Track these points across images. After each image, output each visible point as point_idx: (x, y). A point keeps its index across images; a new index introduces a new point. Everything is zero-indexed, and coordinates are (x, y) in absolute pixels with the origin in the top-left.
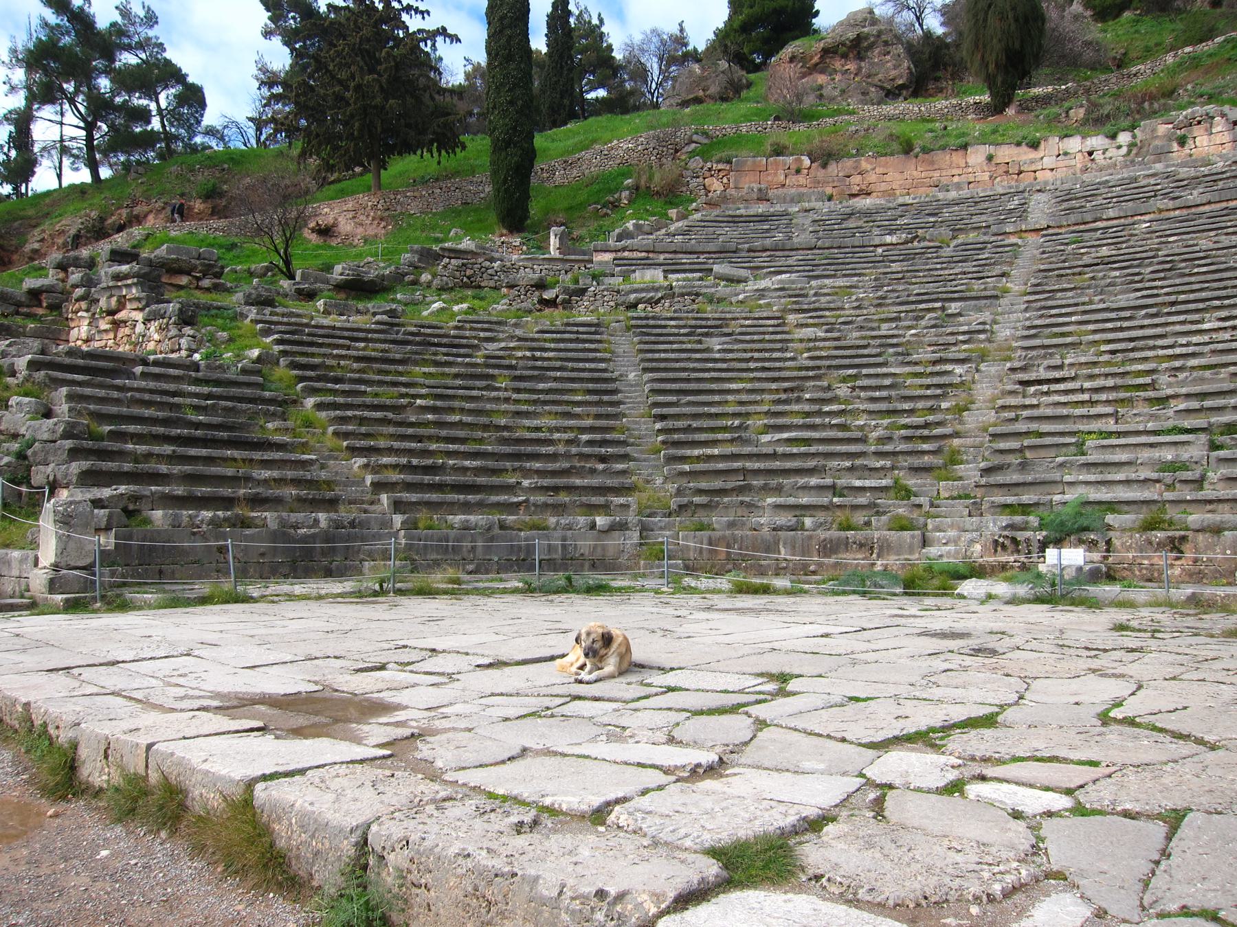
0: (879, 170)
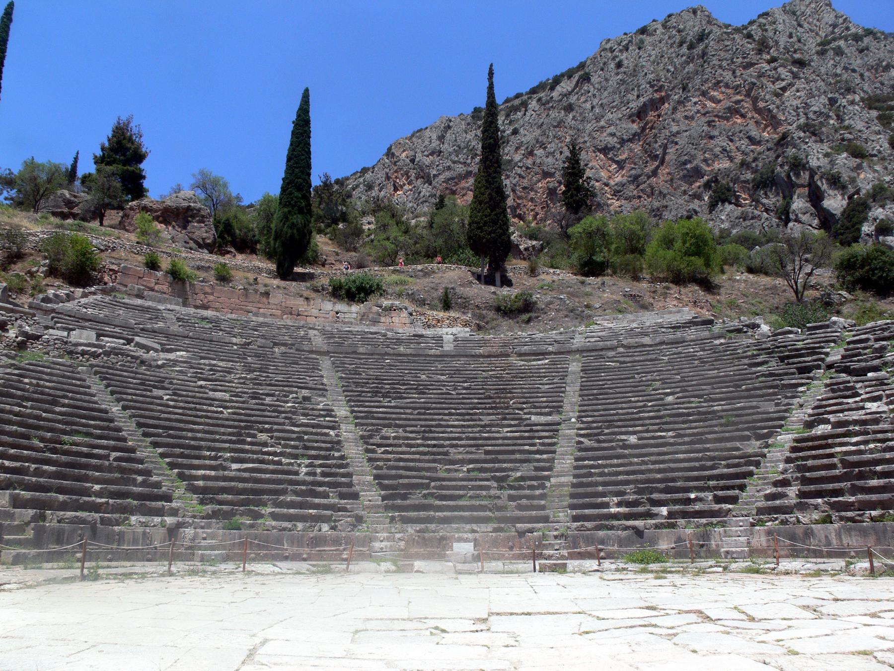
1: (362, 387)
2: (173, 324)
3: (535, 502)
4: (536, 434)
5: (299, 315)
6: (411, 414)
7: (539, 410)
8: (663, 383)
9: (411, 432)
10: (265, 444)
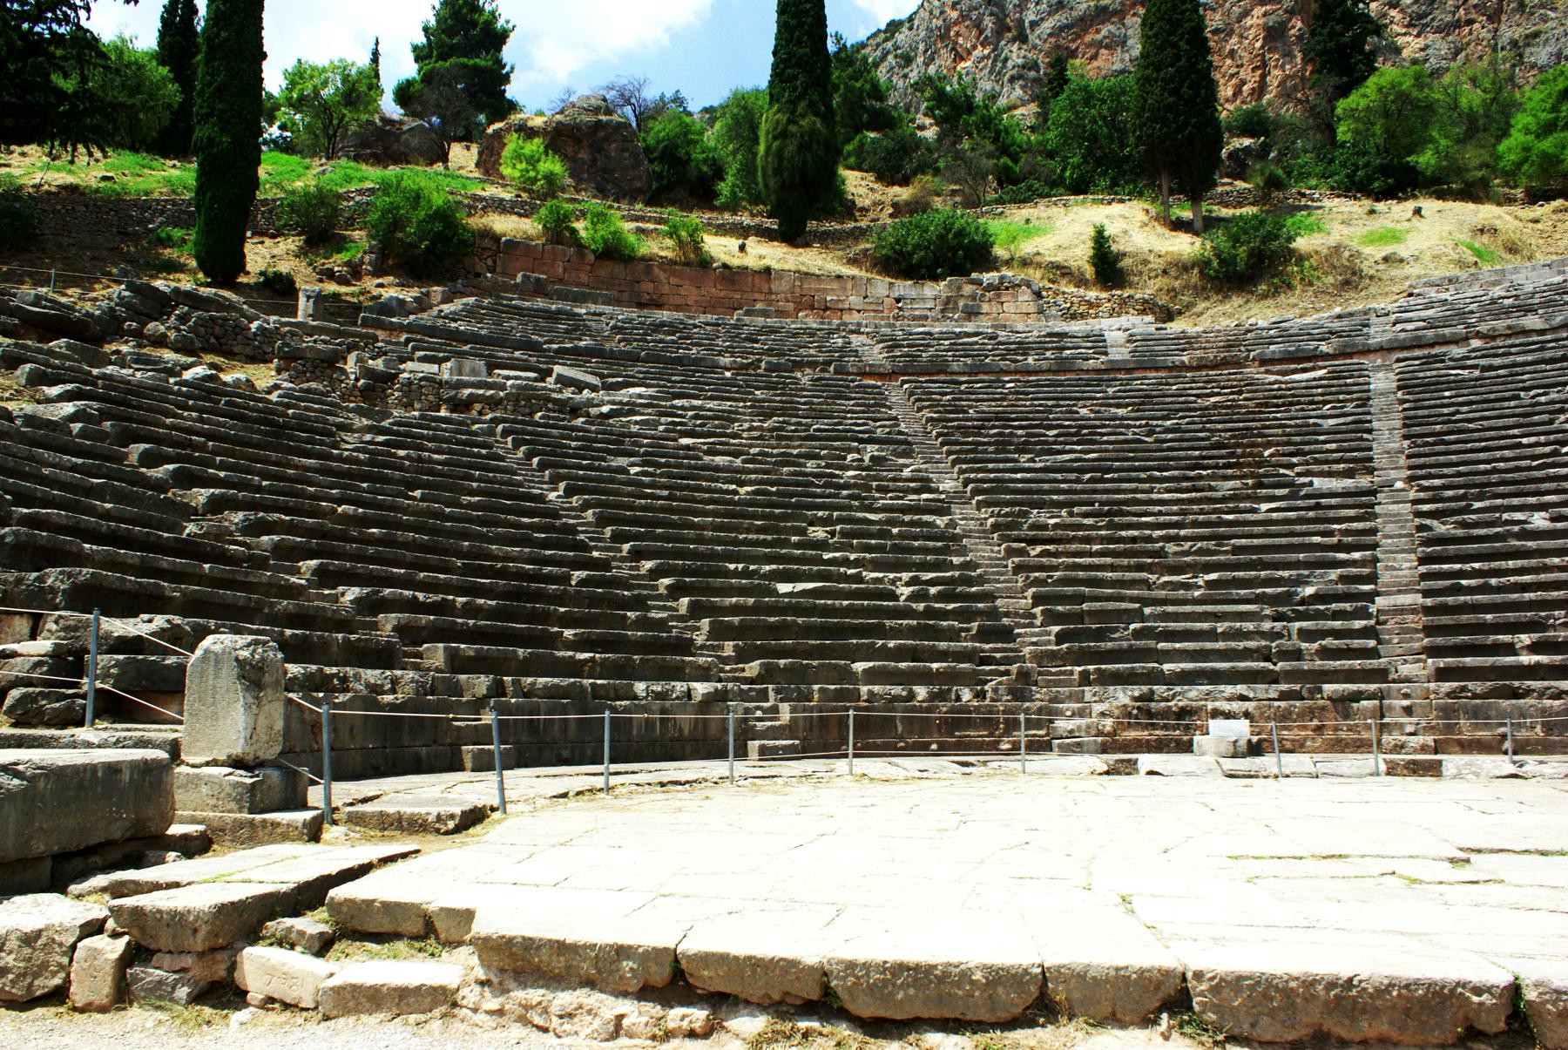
0: (674, 280)
1: (975, 435)
2: (609, 339)
3: (1356, 643)
4: (1331, 514)
5: (826, 309)
6: (1078, 481)
7: (1326, 467)
9: (1086, 515)
10: (823, 545)
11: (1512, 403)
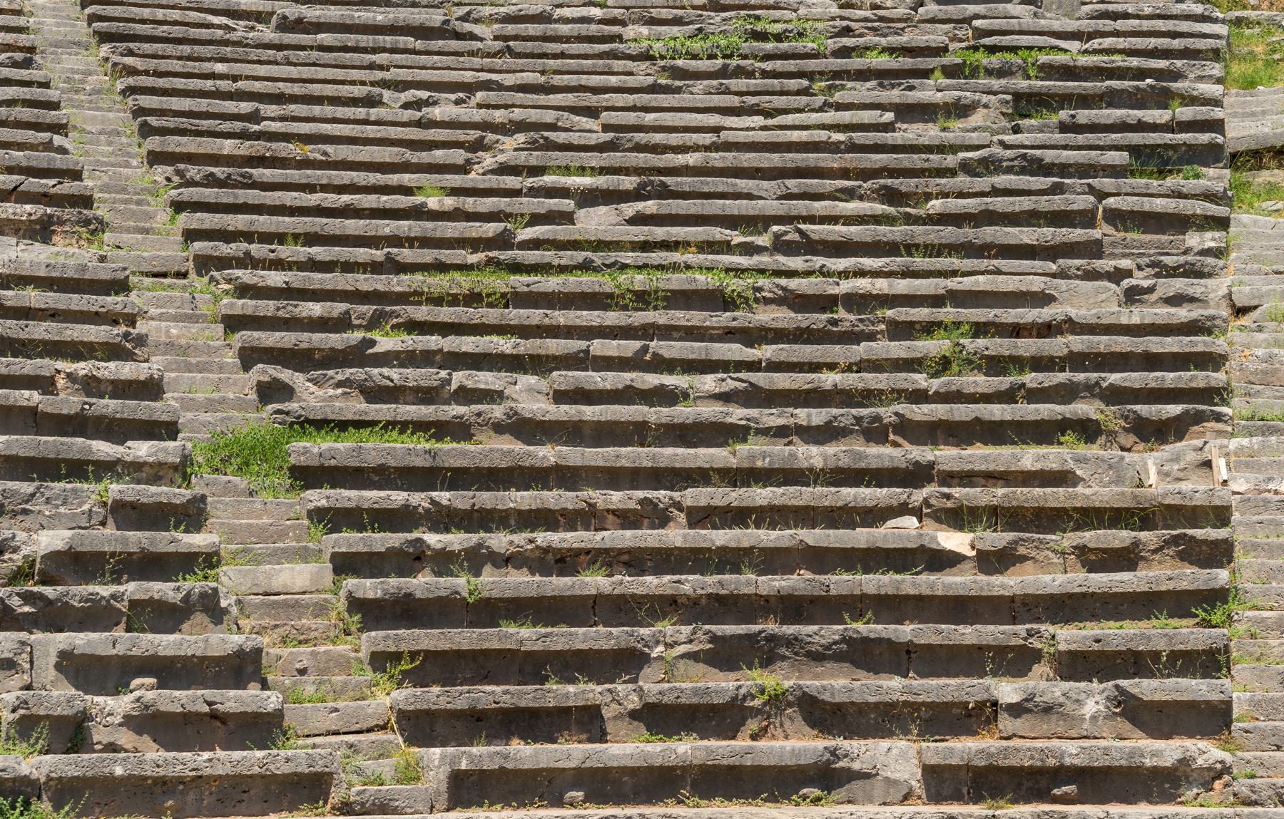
8: (533, 146)
11: (374, 113)
